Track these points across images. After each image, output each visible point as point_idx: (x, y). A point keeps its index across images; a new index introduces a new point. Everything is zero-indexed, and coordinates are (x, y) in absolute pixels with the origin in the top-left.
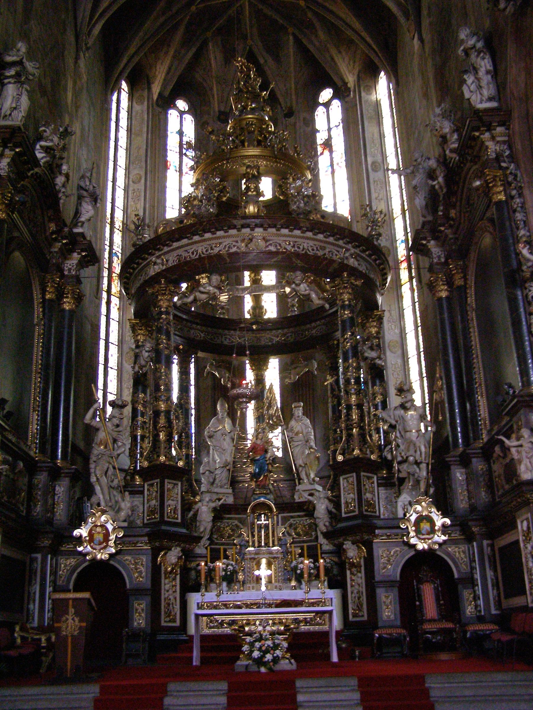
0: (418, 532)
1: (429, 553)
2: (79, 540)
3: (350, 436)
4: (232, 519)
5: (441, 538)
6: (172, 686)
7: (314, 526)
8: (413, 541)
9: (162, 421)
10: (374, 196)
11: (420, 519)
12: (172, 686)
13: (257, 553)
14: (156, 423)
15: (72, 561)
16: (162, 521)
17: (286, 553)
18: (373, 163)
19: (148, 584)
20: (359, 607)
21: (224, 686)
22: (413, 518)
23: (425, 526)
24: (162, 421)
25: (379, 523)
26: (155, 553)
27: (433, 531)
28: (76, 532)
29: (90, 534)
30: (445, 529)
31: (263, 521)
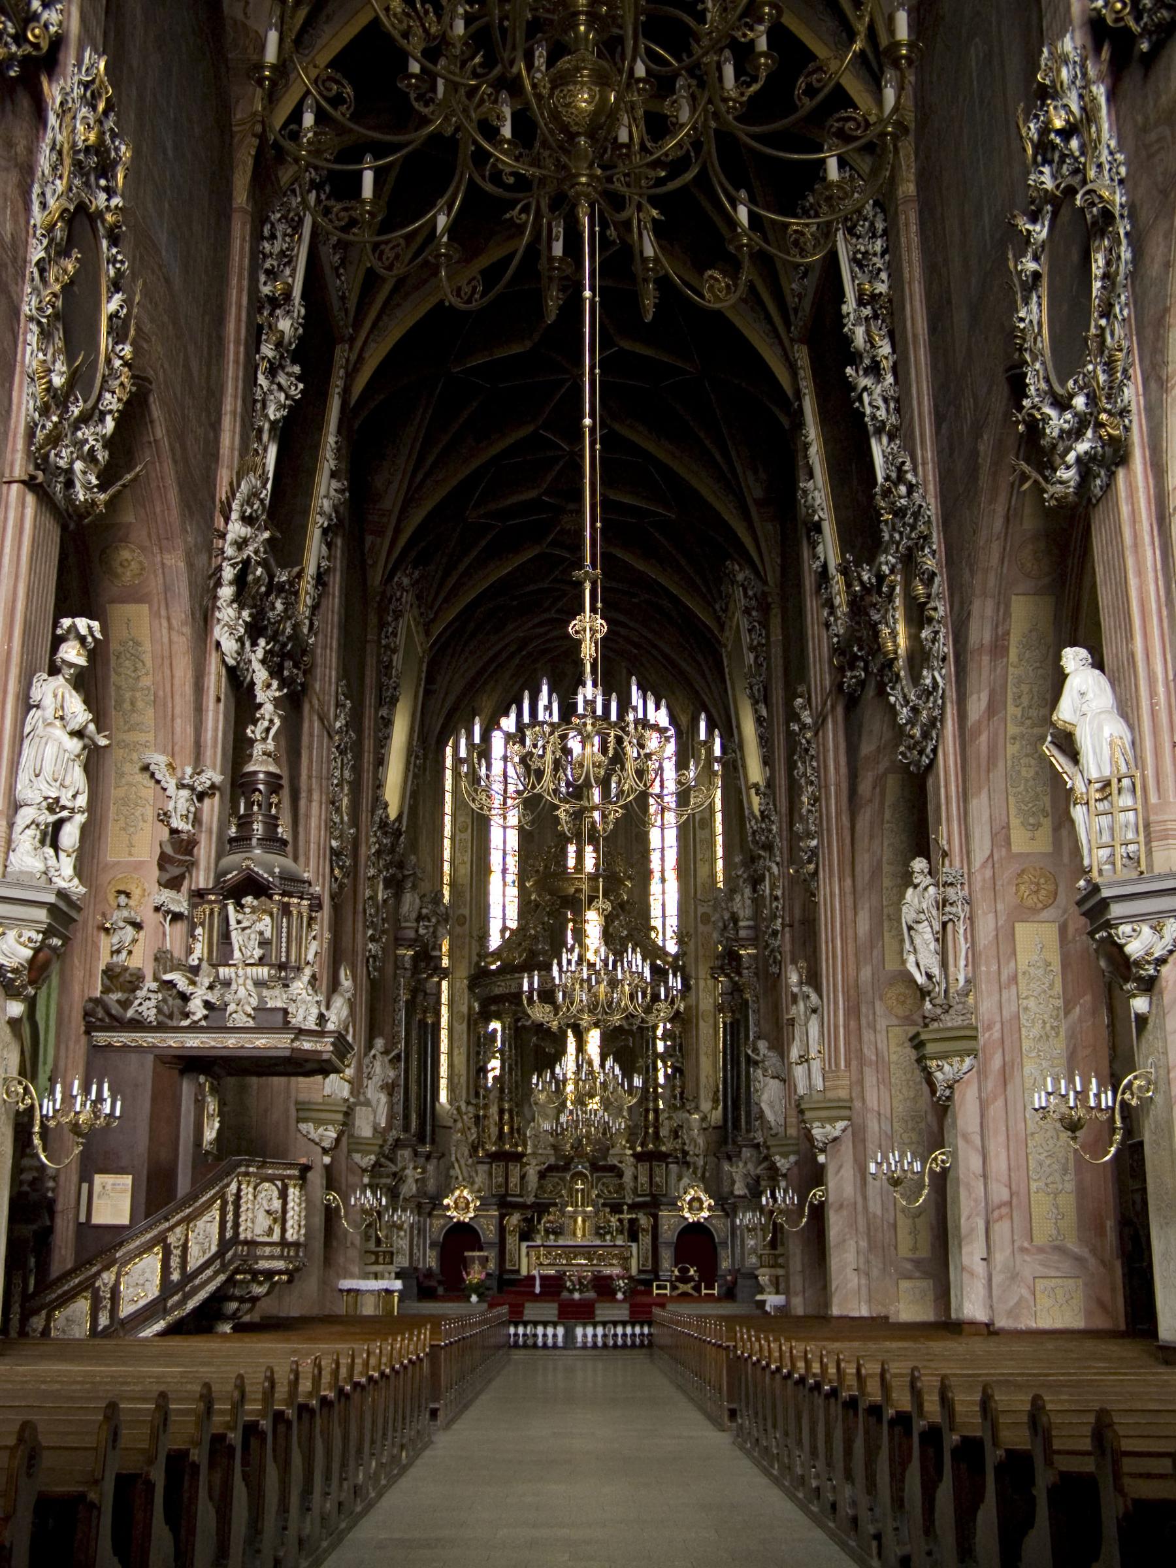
0: (690, 1209)
1: (697, 1225)
2: (448, 1208)
3: (647, 1133)
4: (554, 1178)
5: (706, 1214)
6: (527, 1305)
7: (621, 1187)
8: (687, 1215)
9: (506, 1117)
10: (699, 857)
11: (693, 1199)
12: (527, 1305)
13: (575, 1212)
14: (501, 1118)
15: (442, 1221)
16: (507, 1194)
17: (596, 1213)
18: (701, 820)
19: (496, 1240)
20: (646, 1259)
21: (556, 1305)
22: (688, 1198)
23: (696, 1204)
24: (506, 1117)
25: (664, 1200)
26: (502, 1217)
27: (701, 1209)
28: (446, 1202)
29: (456, 1202)
30: (710, 1208)
31: (580, 1186)
